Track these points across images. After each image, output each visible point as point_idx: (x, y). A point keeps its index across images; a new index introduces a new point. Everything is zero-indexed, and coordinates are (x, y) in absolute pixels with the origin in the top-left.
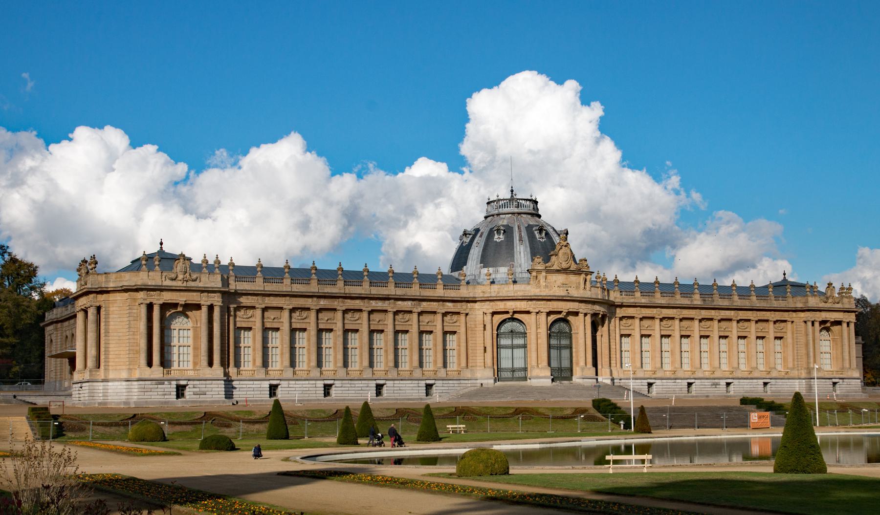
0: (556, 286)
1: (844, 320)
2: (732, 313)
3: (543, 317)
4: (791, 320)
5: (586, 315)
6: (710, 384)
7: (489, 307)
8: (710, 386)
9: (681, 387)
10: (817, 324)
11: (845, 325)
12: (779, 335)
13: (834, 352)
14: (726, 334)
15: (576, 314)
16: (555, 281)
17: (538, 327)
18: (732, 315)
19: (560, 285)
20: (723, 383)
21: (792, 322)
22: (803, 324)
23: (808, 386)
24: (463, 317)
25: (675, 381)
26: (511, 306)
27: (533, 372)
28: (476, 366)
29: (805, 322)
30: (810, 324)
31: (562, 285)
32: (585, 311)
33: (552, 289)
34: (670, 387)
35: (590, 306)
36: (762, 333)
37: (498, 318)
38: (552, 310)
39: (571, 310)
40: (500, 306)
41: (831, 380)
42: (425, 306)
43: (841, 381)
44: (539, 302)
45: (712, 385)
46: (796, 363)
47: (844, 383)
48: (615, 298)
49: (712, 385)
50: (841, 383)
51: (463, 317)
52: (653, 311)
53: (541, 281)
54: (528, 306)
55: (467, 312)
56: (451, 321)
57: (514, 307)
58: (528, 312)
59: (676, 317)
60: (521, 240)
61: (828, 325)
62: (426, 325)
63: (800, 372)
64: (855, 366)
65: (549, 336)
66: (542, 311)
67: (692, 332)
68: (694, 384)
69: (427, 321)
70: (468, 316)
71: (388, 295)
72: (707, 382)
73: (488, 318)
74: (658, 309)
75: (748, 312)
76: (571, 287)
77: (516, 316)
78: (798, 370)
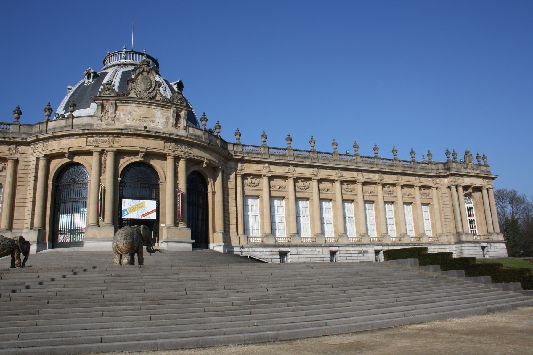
1: (484, 186)
2: (377, 176)
3: (109, 160)
4: (436, 186)
5: (177, 159)
6: (356, 252)
8: (356, 255)
9: (322, 256)
10: (460, 189)
11: (485, 191)
12: (425, 201)
13: (478, 218)
14: (372, 199)
15: (163, 157)
17: (102, 171)
18: (376, 178)
20: (371, 249)
21: (437, 188)
22: (448, 190)
23: (459, 251)
24: (10, 166)
25: (314, 249)
28: (22, 228)
29: (449, 187)
30: (454, 189)
32: (177, 153)
34: (309, 256)
35: (183, 148)
36: (408, 199)
37: (56, 164)
40: (54, 146)
41: (480, 245)
43: (489, 245)
44: (105, 139)
45: (359, 253)
46: (444, 229)
47: (492, 247)
49: (359, 253)
50: (489, 247)
52: (285, 170)
53: (110, 112)
58: (89, 153)
59: (313, 177)
61: (470, 190)
63: (449, 237)
64: (499, 231)
66: (107, 148)
67: (334, 195)
68: (338, 253)
70: (20, 163)
72: (354, 250)
73: (42, 163)
74: (291, 167)
75: (393, 176)
76: (153, 122)
78: (447, 236)
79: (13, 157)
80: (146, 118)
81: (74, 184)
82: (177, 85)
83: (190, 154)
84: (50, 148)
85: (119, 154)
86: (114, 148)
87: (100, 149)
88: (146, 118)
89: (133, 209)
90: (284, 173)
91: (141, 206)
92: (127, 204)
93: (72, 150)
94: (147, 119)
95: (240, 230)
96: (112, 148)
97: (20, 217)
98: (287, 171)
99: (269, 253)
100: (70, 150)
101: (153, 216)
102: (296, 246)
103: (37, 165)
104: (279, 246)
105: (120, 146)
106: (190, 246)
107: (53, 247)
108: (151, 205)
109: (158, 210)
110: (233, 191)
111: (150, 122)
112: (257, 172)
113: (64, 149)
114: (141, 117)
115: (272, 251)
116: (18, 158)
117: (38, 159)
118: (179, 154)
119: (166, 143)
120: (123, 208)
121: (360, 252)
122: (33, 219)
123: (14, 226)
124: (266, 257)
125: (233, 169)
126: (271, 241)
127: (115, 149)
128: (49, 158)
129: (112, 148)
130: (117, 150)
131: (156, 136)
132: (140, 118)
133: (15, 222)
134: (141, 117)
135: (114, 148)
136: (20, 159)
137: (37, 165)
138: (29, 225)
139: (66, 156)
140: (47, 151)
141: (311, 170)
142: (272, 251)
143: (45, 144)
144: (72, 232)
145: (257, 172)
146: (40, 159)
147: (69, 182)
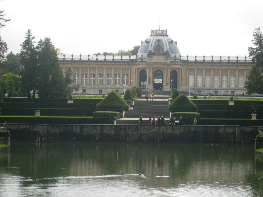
3: (151, 70)
7: (136, 67)
24: (129, 70)
26: (141, 66)
37: (140, 70)
51: (129, 70)
60: (151, 45)
66: (150, 67)
73: (136, 70)
85: (153, 68)
87: (149, 67)
89: (157, 81)
91: (159, 80)
92: (155, 80)
101: (162, 82)
102: (204, 89)
108: (161, 80)
109: (163, 81)
117: (135, 69)
120: (155, 81)
121: (225, 92)
122: (135, 83)
126: (196, 88)
128: (138, 68)
131: (161, 63)
141: (211, 66)
144: (144, 86)
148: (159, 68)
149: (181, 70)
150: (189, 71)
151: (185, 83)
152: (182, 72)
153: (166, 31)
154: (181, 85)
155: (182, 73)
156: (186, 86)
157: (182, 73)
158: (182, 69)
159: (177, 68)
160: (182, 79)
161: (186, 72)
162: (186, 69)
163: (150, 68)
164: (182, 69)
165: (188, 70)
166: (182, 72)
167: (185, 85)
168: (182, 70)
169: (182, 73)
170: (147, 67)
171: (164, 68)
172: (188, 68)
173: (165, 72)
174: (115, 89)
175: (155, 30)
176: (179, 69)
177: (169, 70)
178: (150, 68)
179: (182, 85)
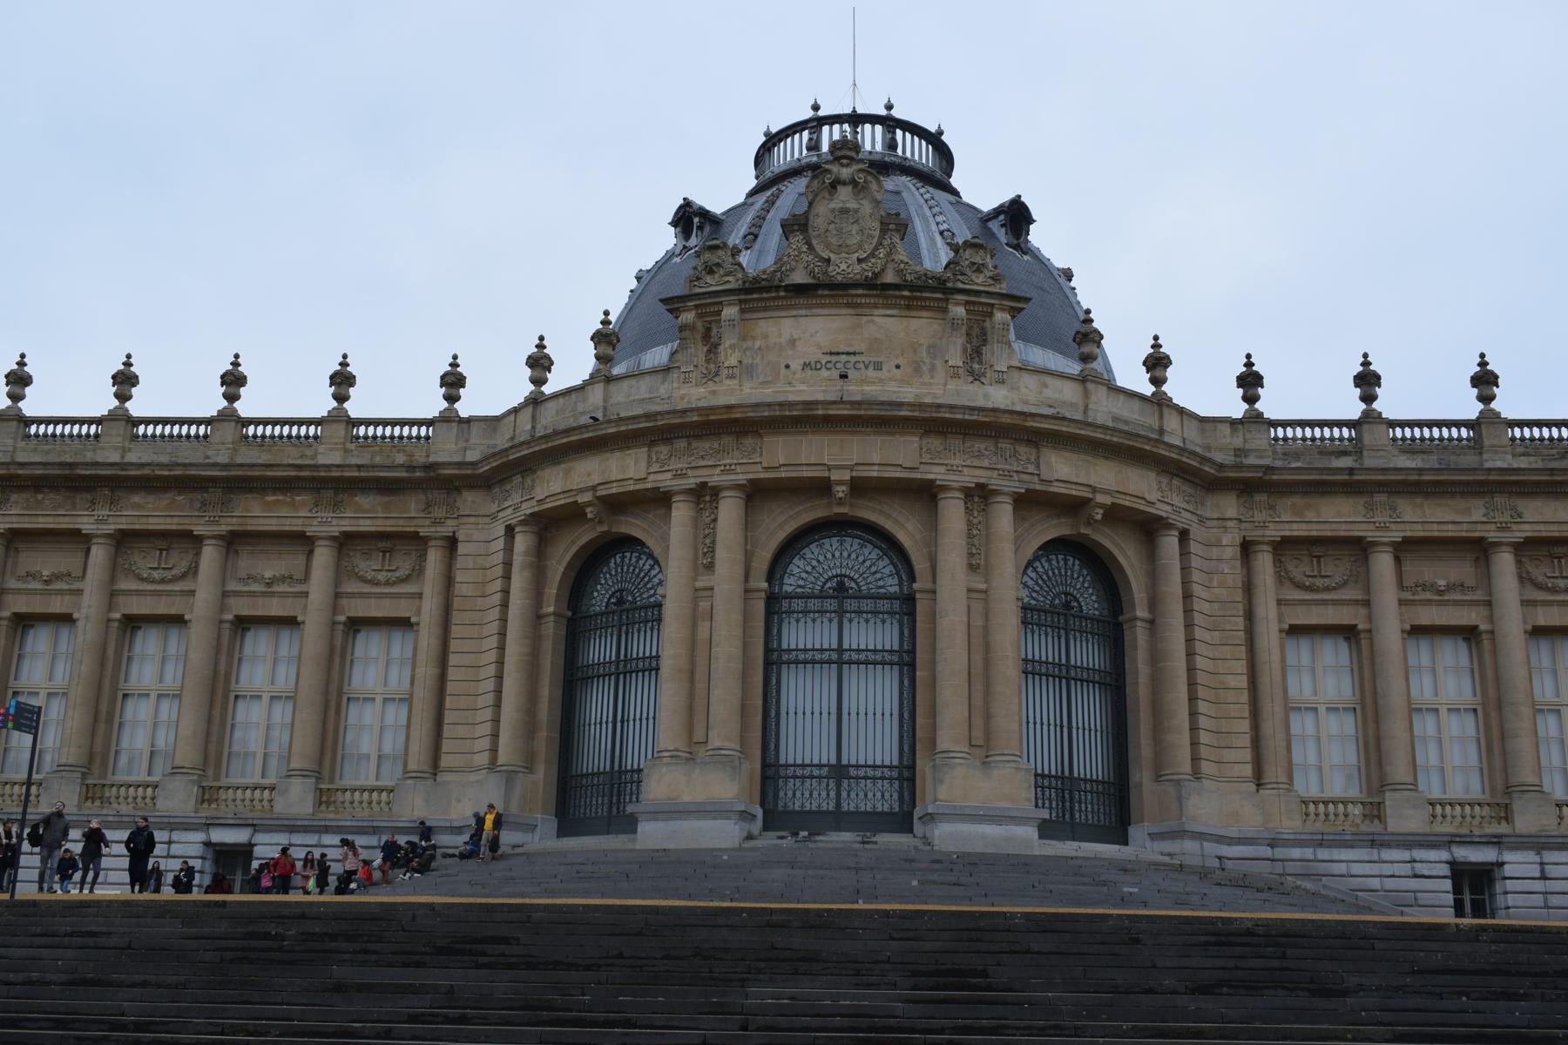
0: (796, 365)
7: (520, 502)
16: (792, 342)
19: (814, 355)
24: (434, 558)
27: (660, 785)
31: (825, 359)
32: (969, 478)
33: (778, 373)
38: (762, 476)
39: (874, 472)
42: (260, 514)
48: (1239, 452)
51: (434, 558)
54: (655, 468)
55: (446, 529)
56: (381, 577)
57: (596, 479)
62: (264, 594)
65: (775, 605)
66: (716, 478)
69: (268, 574)
70: (462, 548)
71: (71, 465)
73: (522, 542)
76: (878, 366)
77: (632, 526)
79: (439, 529)
80: (848, 354)
81: (622, 611)
82: (1002, 217)
83: (1025, 477)
84: (539, 493)
85: (757, 494)
86: (740, 477)
87: (691, 482)
88: (848, 354)
90: (1465, 527)
93: (604, 493)
94: (852, 359)
95: (1273, 773)
96: (732, 477)
97: (460, 731)
98: (1477, 515)
99: (1406, 869)
100: (598, 494)
103: (509, 548)
104: (1450, 841)
105: (759, 468)
106: (1031, 832)
107: (562, 832)
110: (1235, 613)
111: (866, 367)
112: (1335, 526)
113: (581, 491)
114: (831, 353)
115: (1415, 861)
116: (454, 533)
117: (510, 531)
118: (982, 481)
119: (925, 441)
123: (445, 761)
124: (1390, 884)
125: (1230, 524)
127: (741, 478)
128: (547, 524)
129: (732, 477)
130: (751, 481)
132: (828, 358)
133: (446, 746)
134: (831, 353)
135: (740, 477)
136: (460, 536)
137: (509, 548)
138: (483, 759)
139: (589, 516)
140: (534, 502)
142: (1415, 861)
143: (529, 481)
145: (1335, 526)
146: (517, 529)
147: (606, 607)
148: (861, 488)
149: (1170, 543)
150: (1282, 578)
151: (1246, 740)
152: (1186, 583)
153: (944, 155)
154: (1187, 767)
155: (1197, 590)
156: (1259, 780)
157: (1187, 596)
158: (1184, 535)
159: (1118, 516)
160: (1192, 684)
161: (1249, 588)
162: (1247, 548)
163: (704, 495)
164: (1184, 535)
165: (1264, 563)
166: (1196, 576)
167: (1248, 770)
168: (1184, 553)
169: (1187, 596)
170: (665, 481)
171: (925, 494)
172: (1274, 532)
173: (953, 557)
174: (200, 836)
175: (809, 114)
176: (1148, 528)
177: (1003, 517)
178: (704, 495)
179: (1196, 774)
